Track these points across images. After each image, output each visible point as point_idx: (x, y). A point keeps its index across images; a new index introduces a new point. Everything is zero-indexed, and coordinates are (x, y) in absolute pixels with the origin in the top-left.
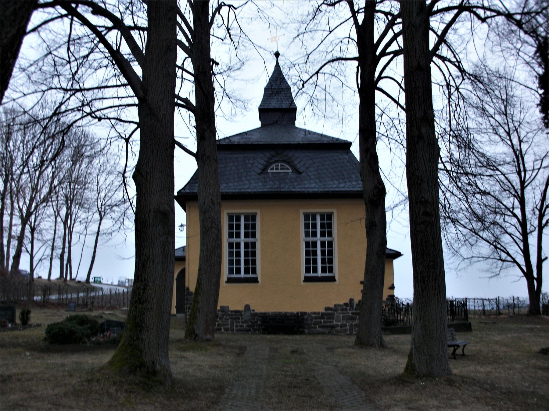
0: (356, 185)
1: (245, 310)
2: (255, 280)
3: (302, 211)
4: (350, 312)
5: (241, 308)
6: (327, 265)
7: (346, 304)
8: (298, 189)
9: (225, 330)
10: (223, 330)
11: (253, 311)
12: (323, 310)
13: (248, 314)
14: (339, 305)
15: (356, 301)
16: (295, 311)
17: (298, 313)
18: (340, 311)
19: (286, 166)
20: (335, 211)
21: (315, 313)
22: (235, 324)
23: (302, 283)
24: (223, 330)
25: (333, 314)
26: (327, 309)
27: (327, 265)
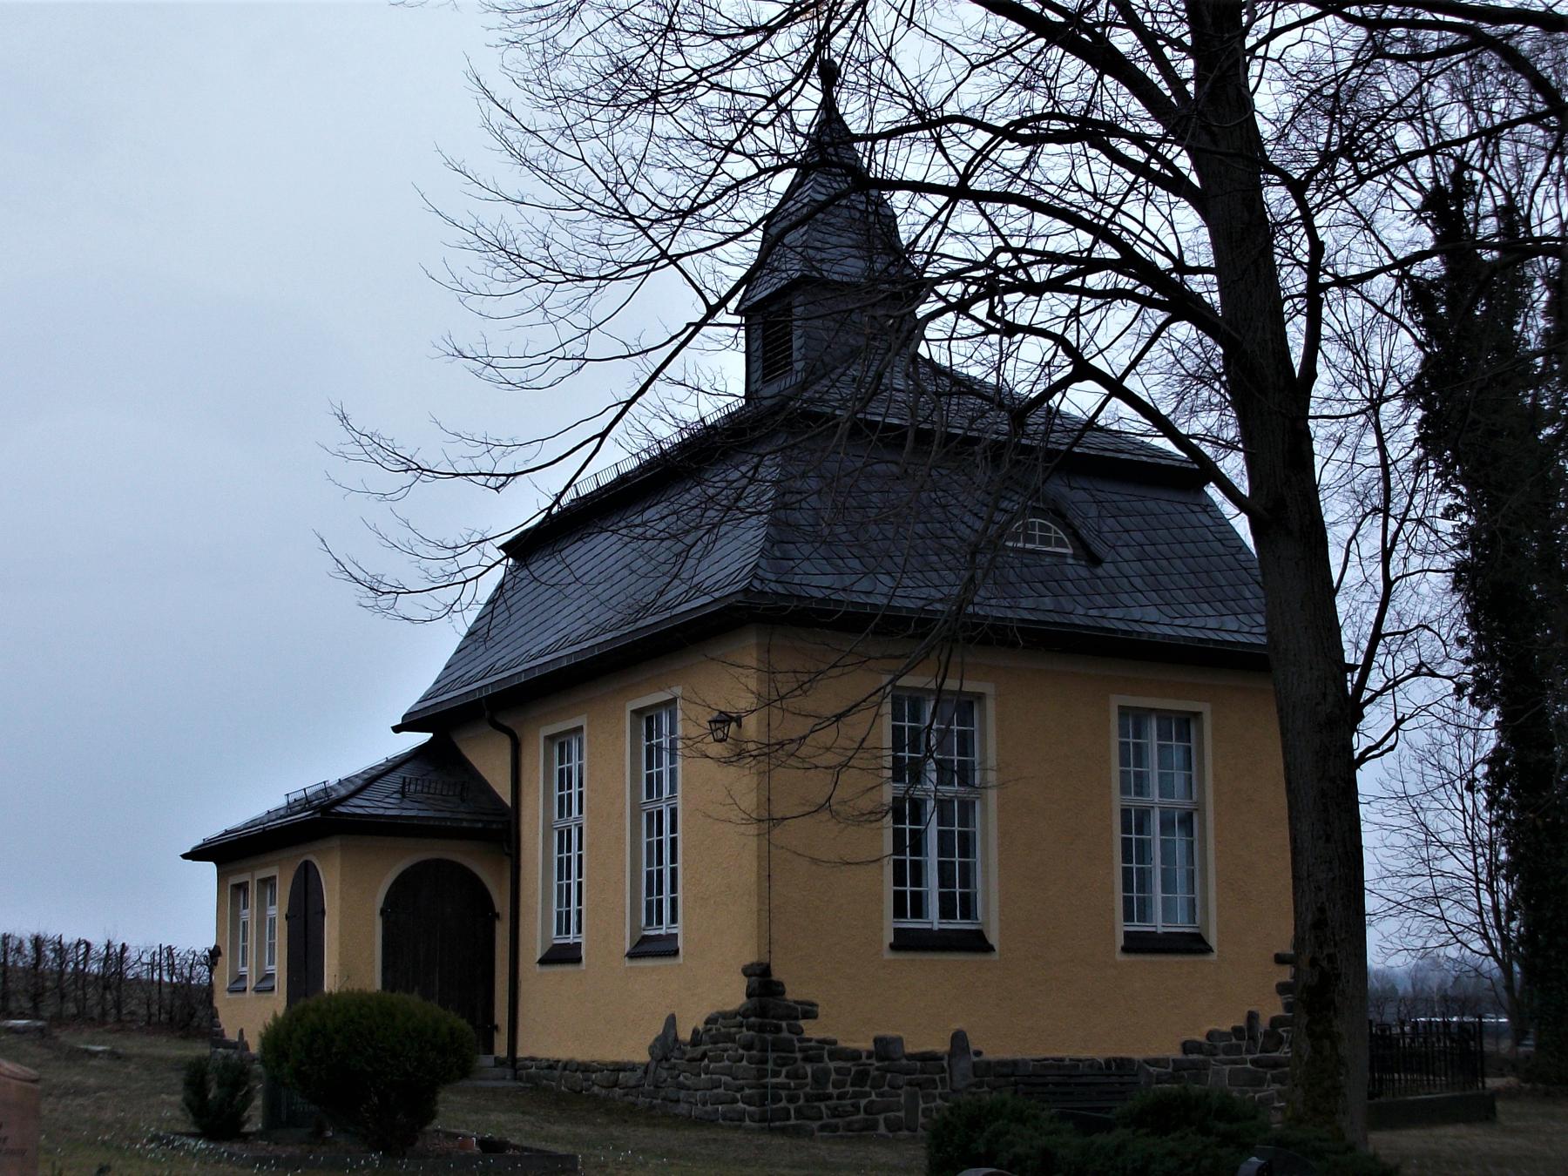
0: (1243, 627)
1: (951, 1055)
2: (976, 943)
3: (1116, 701)
4: (1249, 1057)
5: (941, 1045)
6: (1135, 895)
7: (1237, 1031)
8: (1080, 614)
9: (894, 1126)
10: (882, 1129)
11: (978, 1053)
12: (1175, 1053)
13: (963, 1065)
14: (1223, 1035)
15: (1264, 1023)
16: (1099, 1052)
17: (1108, 1062)
18: (1222, 1057)
19: (1057, 532)
20: (1204, 707)
21: (1155, 1062)
22: (922, 1105)
23: (889, 955)
24: (882, 1129)
25: (1204, 1066)
26: (1188, 1047)
27: (958, 890)
